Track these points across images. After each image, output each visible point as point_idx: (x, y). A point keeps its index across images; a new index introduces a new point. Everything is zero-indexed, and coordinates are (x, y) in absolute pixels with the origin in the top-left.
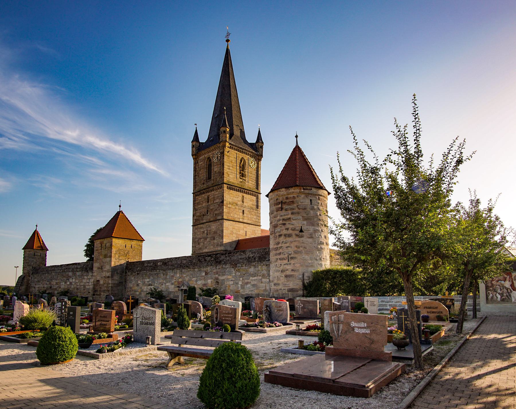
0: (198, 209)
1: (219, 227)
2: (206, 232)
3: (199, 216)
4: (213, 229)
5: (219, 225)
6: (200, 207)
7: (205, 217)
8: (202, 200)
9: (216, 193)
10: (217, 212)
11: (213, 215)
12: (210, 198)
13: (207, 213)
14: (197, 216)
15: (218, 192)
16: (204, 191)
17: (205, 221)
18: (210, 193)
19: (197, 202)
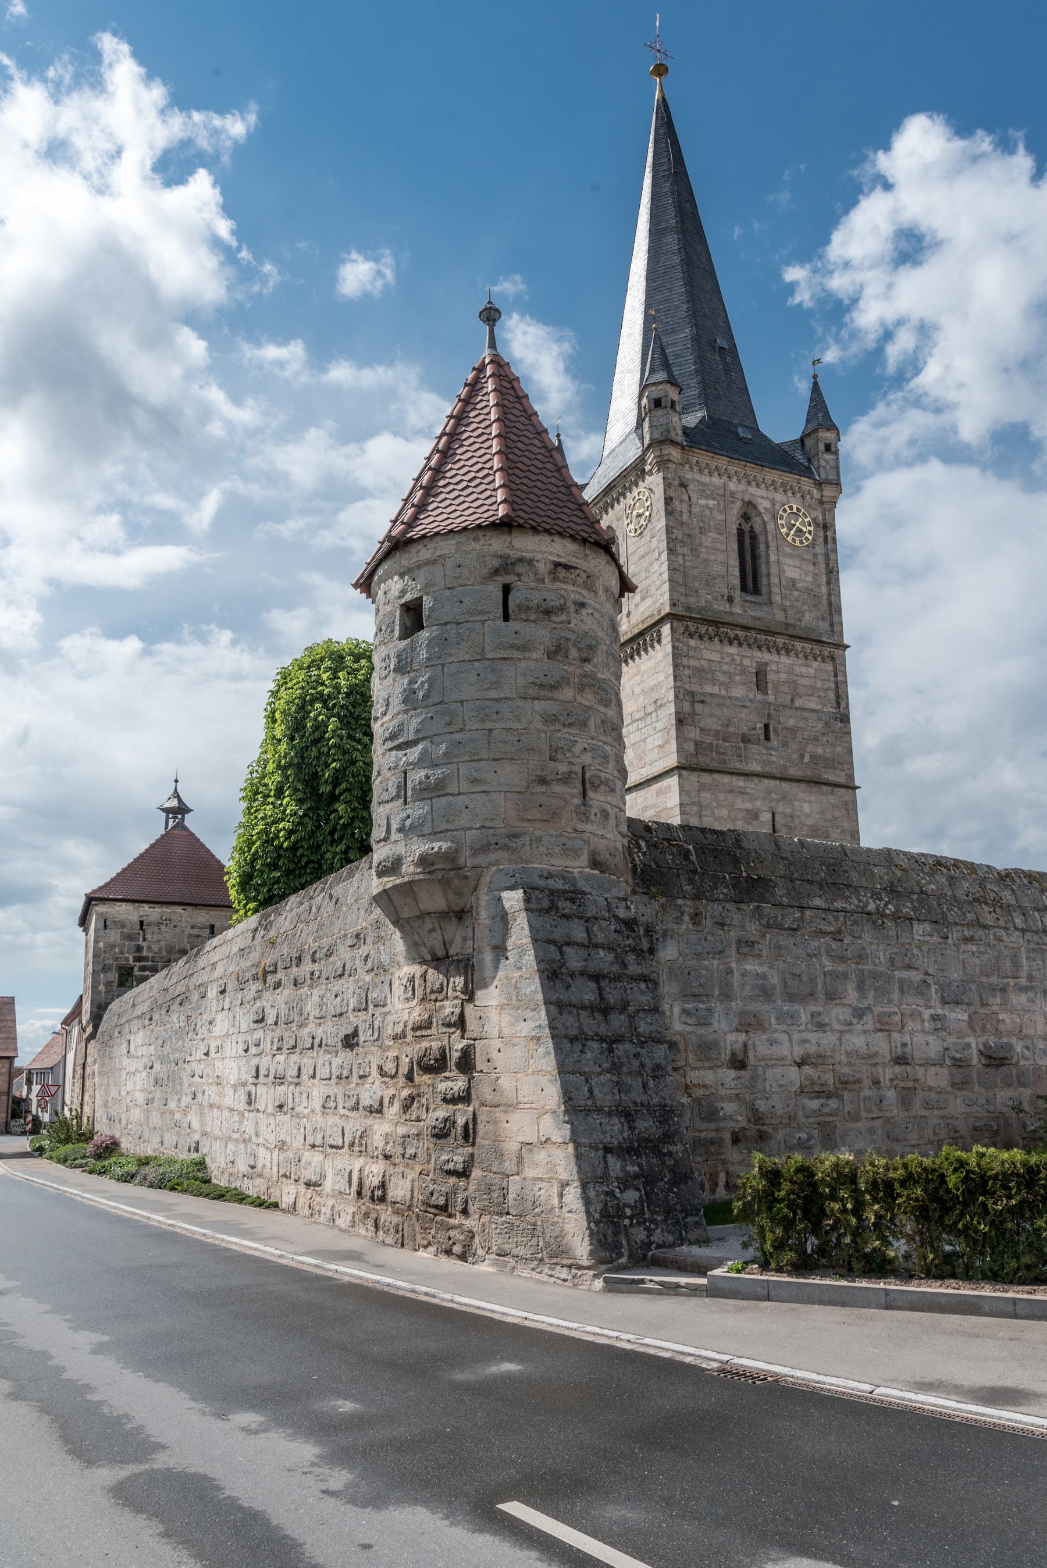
0: (708, 699)
1: (837, 814)
2: (766, 817)
3: (718, 731)
4: (808, 816)
5: (833, 806)
6: (711, 695)
7: (754, 748)
8: (725, 667)
9: (804, 670)
10: (820, 750)
11: (802, 756)
12: (771, 677)
13: (767, 738)
14: (702, 730)
15: (812, 671)
16: (741, 634)
17: (758, 768)
18: (775, 658)
19: (693, 663)
